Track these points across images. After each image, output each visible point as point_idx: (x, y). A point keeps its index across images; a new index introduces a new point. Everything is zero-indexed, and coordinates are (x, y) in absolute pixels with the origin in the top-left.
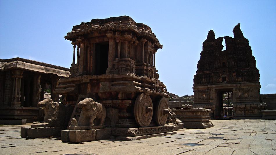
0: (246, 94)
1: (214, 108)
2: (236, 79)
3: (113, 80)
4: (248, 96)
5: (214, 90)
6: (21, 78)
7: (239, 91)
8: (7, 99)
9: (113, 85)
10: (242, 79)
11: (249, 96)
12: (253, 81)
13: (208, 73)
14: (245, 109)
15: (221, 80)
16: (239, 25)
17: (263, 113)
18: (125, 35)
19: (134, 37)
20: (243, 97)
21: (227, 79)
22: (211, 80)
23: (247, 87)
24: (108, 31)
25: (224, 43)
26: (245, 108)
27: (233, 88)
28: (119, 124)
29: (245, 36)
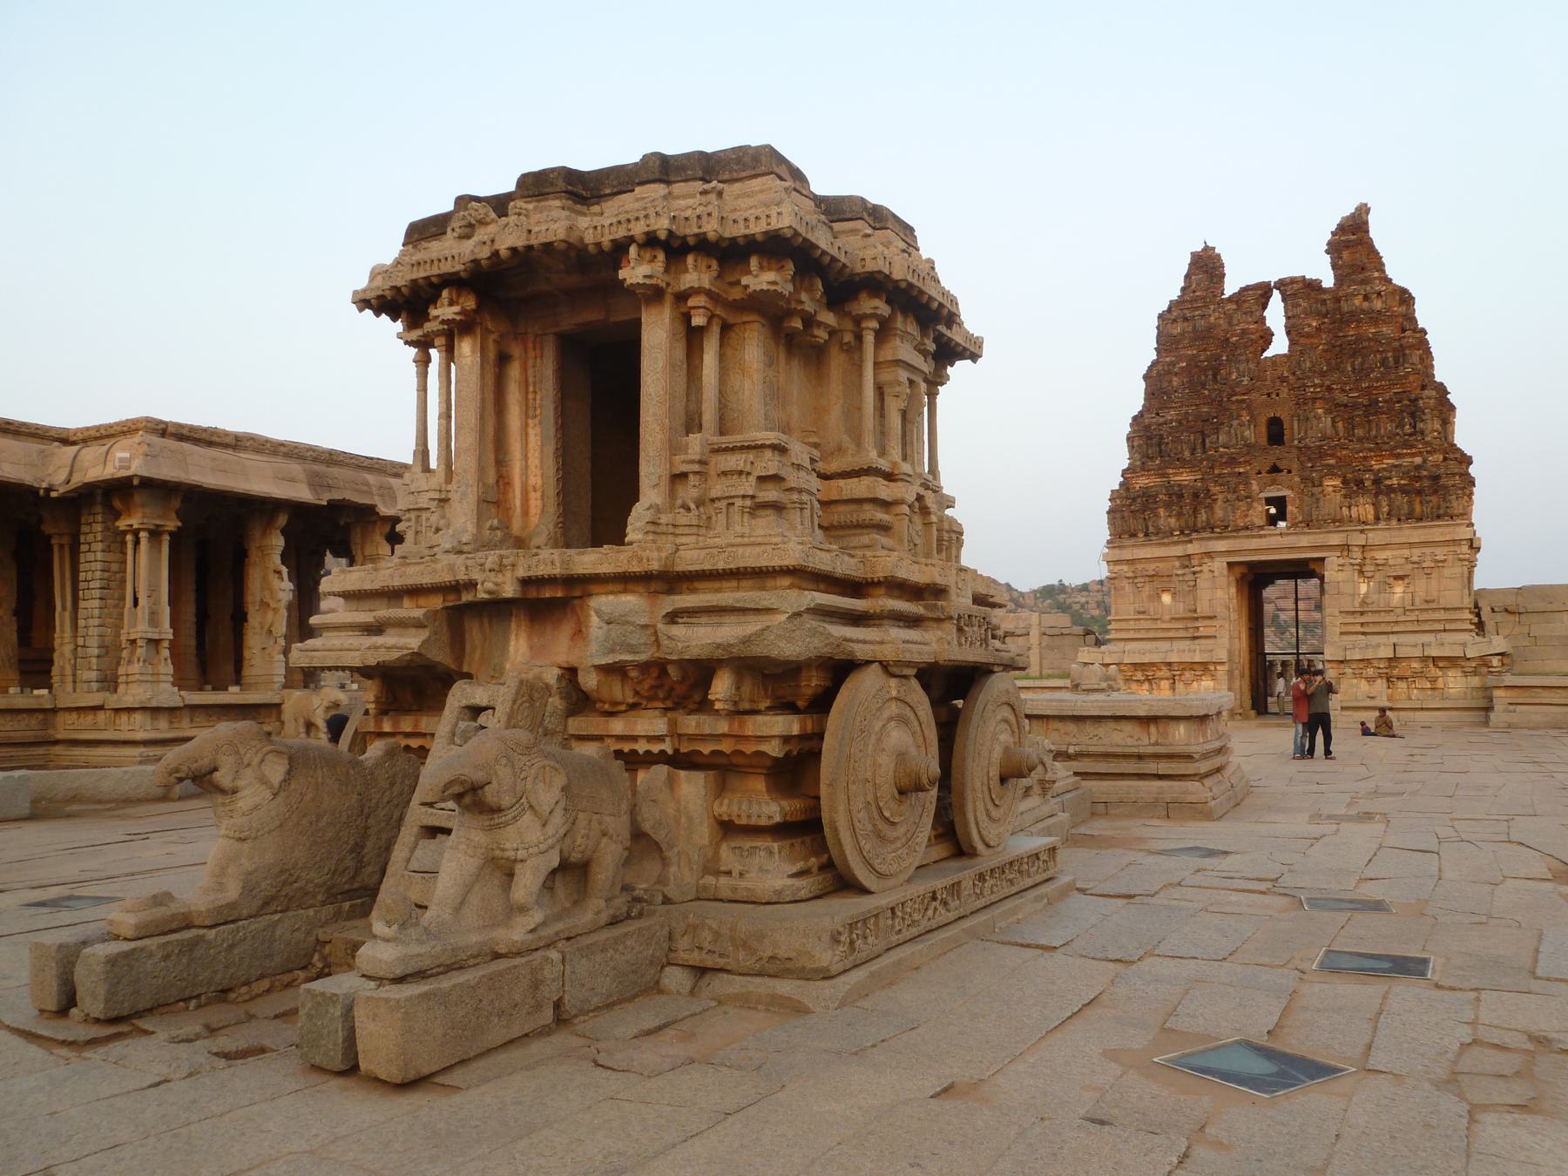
0: (1399, 589)
3: (669, 581)
5: (1219, 565)
6: (171, 534)
7: (1361, 572)
8: (96, 652)
9: (673, 617)
10: (1376, 506)
12: (1439, 517)
13: (1185, 477)
14: (1395, 672)
15: (1258, 513)
16: (1362, 212)
17: (1497, 693)
18: (749, 272)
19: (810, 290)
21: (1289, 508)
22: (1203, 516)
24: (633, 250)
25: (1275, 314)
26: (1393, 660)
27: (1323, 560)
28: (723, 880)
29: (1398, 271)
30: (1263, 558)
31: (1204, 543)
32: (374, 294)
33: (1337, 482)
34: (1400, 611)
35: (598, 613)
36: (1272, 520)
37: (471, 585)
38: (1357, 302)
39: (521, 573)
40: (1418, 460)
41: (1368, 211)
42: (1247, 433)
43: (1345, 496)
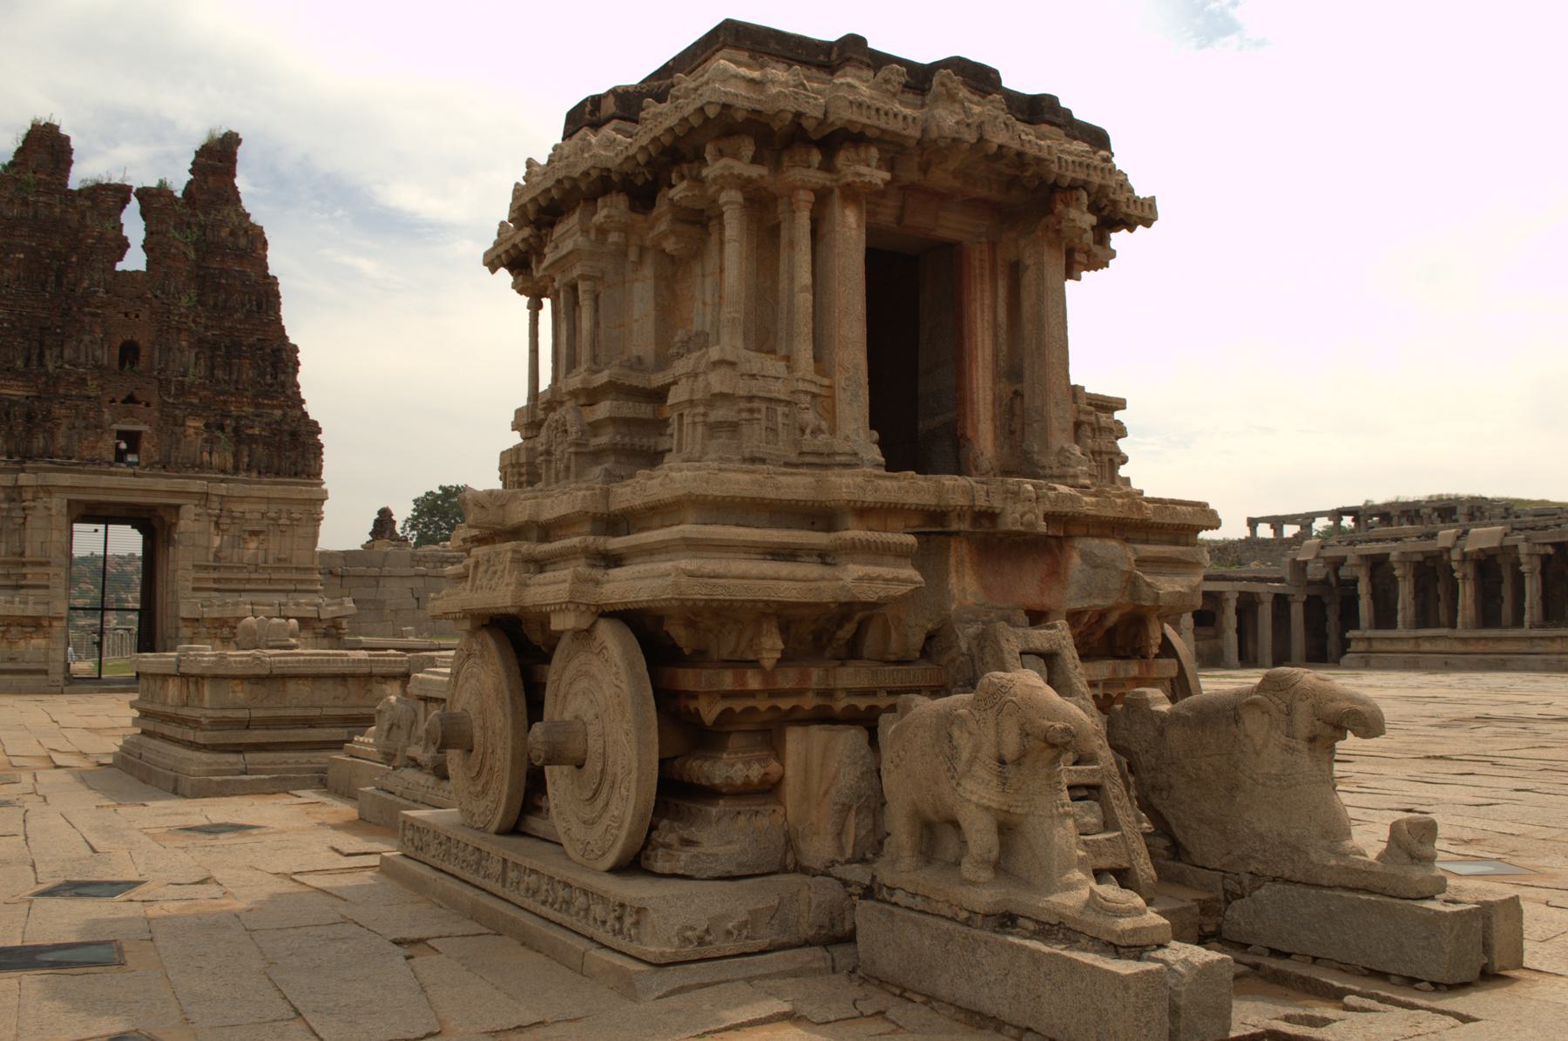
0: (253, 545)
1: (61, 619)
2: (206, 456)
4: (261, 554)
5: (58, 503)
7: (217, 524)
10: (236, 455)
11: (271, 558)
12: (296, 475)
20: (235, 559)
21: (145, 445)
22: (39, 443)
23: (263, 507)
25: (133, 225)
27: (177, 507)
30: (112, 498)
31: (41, 474)
32: (747, 104)
33: (200, 424)
34: (252, 568)
35: (1087, 557)
36: (120, 456)
37: (991, 516)
38: (224, 233)
39: (1048, 507)
40: (278, 413)
41: (239, 142)
42: (98, 353)
43: (206, 441)
